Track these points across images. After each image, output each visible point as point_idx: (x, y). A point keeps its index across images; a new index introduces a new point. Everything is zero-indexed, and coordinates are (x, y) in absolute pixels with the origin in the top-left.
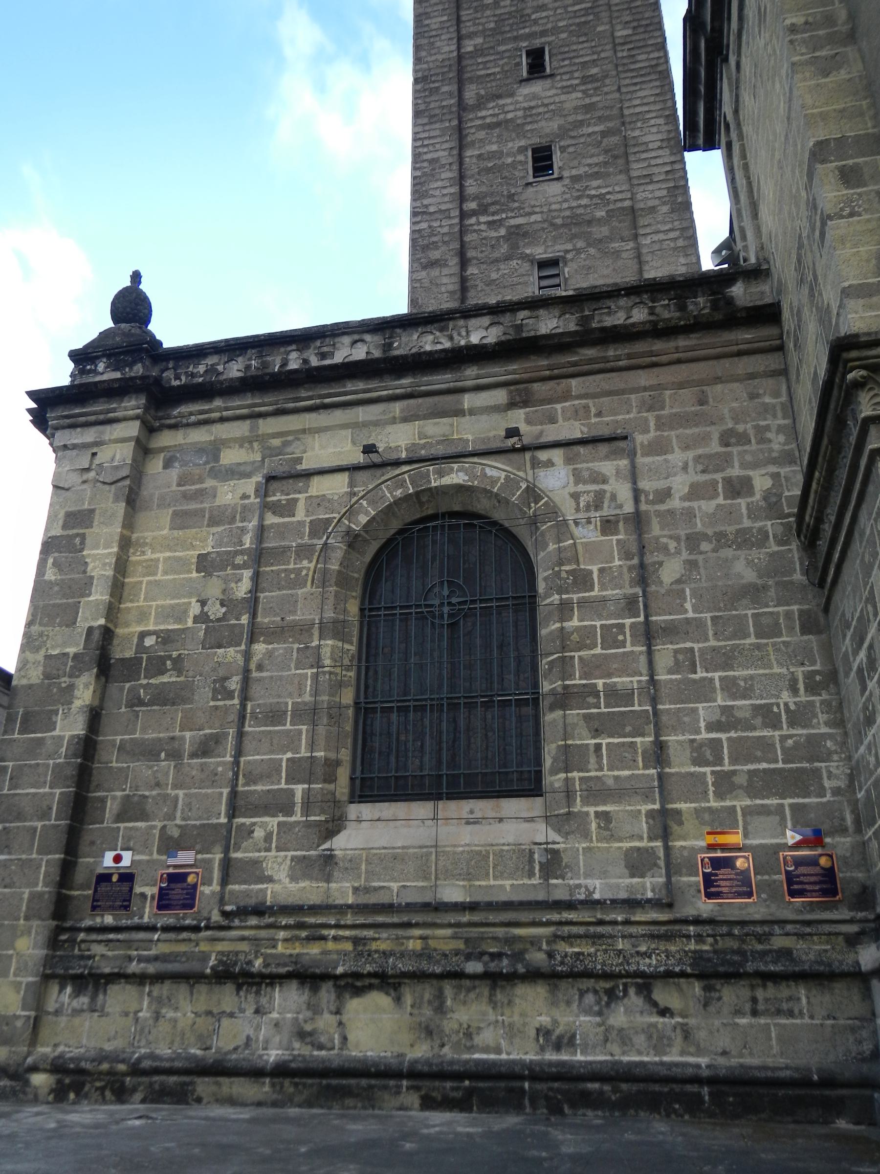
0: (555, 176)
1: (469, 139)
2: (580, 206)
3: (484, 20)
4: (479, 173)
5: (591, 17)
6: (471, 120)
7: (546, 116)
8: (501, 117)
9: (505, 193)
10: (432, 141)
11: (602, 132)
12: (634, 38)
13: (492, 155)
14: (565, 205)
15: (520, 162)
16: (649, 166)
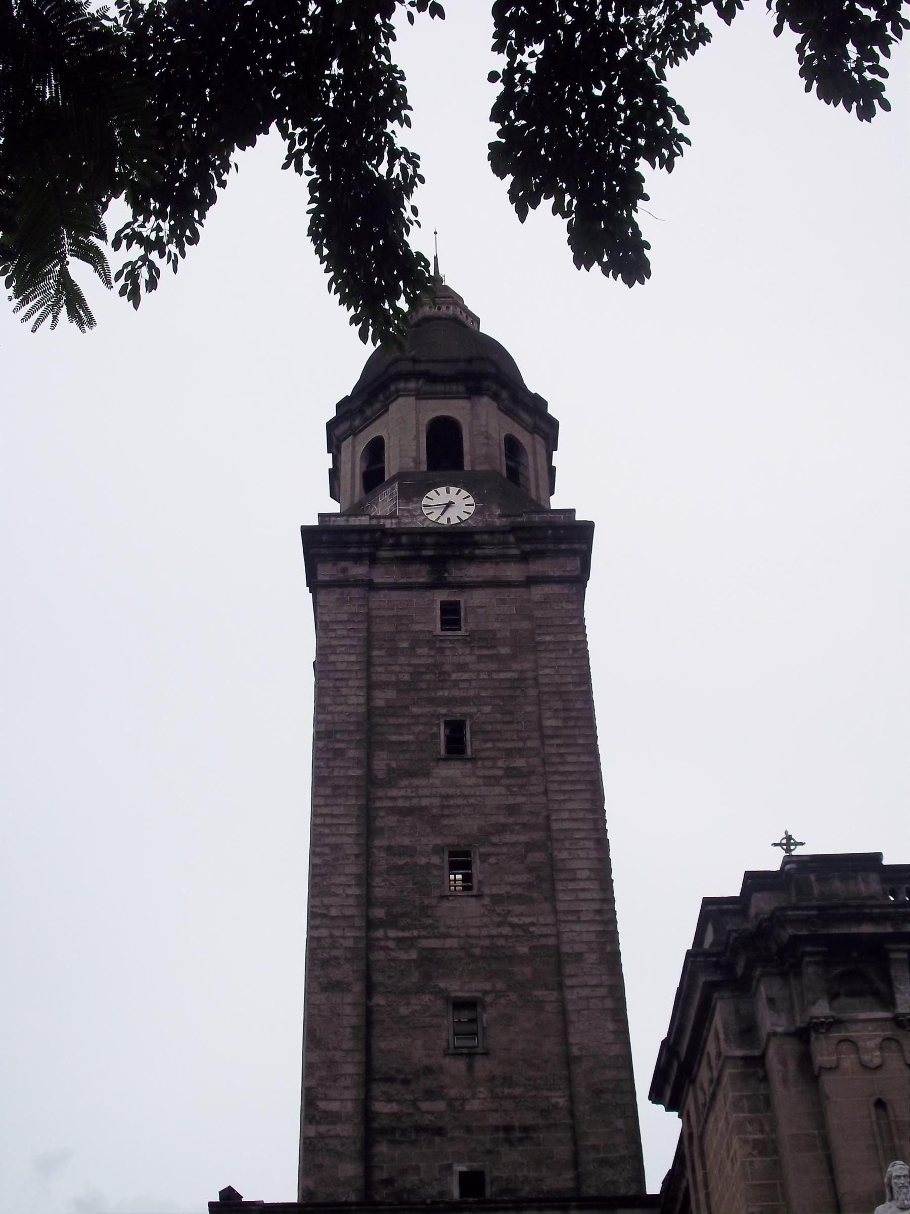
0: (475, 892)
1: (379, 823)
2: (500, 936)
3: (397, 669)
4: (388, 872)
5: (518, 692)
6: (380, 798)
7: (467, 810)
8: (415, 802)
9: (417, 903)
10: (335, 821)
11: (527, 844)
12: (565, 732)
13: (403, 851)
14: (484, 932)
15: (435, 866)
16: (577, 900)
